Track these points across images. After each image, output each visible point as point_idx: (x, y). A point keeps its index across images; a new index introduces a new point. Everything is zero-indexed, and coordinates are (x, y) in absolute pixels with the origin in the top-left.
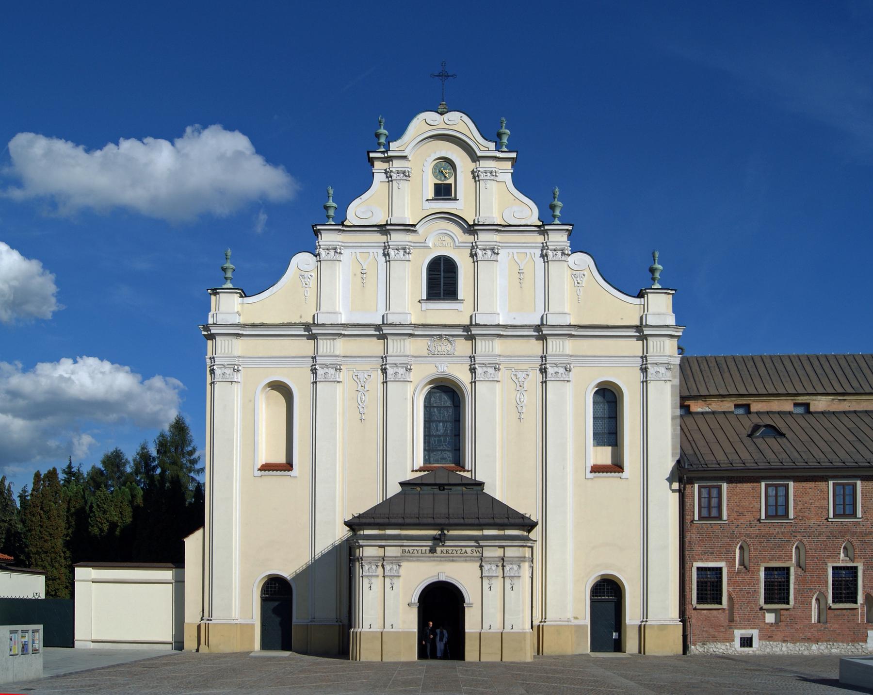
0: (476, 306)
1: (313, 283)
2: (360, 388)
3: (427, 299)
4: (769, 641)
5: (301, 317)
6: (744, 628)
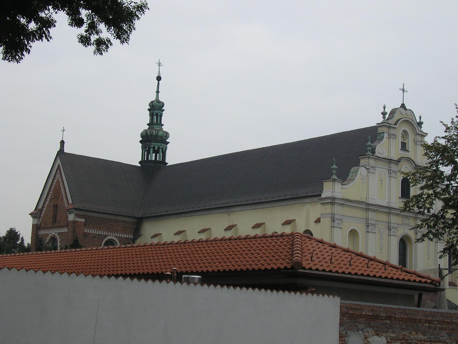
3: (401, 197)
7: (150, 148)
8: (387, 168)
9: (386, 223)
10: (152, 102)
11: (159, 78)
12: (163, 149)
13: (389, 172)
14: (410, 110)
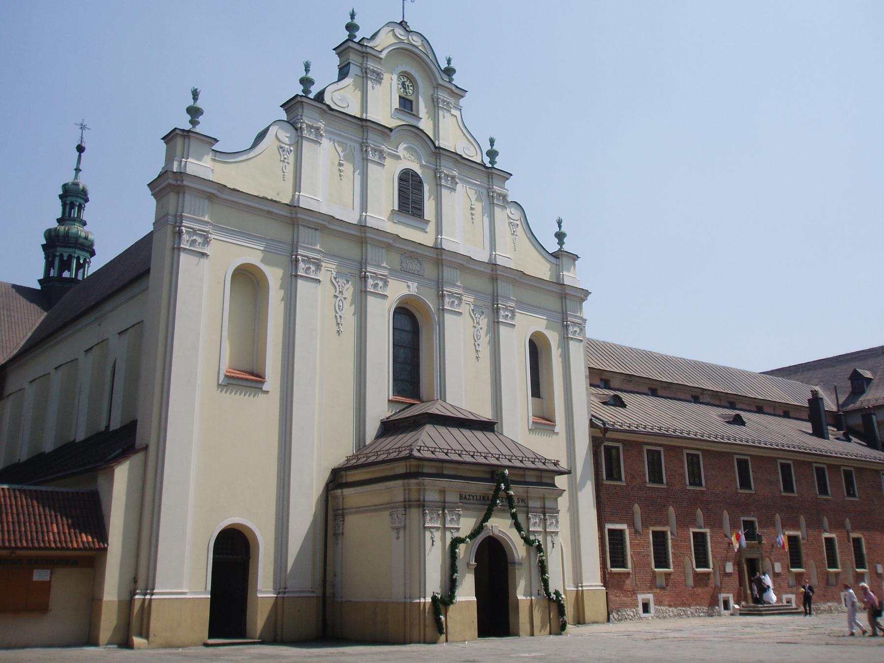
0: (439, 230)
1: (291, 158)
2: (337, 294)
4: (660, 606)
5: (278, 194)
6: (644, 593)
7: (54, 256)
8: (357, 139)
9: (354, 261)
10: (65, 186)
11: (80, 149)
12: (78, 259)
13: (362, 150)
14: (420, 34)
